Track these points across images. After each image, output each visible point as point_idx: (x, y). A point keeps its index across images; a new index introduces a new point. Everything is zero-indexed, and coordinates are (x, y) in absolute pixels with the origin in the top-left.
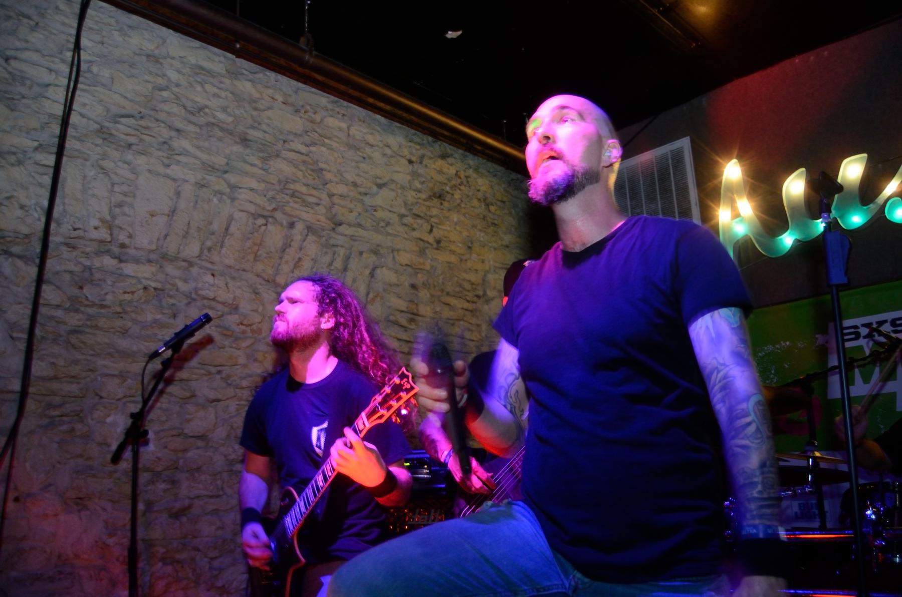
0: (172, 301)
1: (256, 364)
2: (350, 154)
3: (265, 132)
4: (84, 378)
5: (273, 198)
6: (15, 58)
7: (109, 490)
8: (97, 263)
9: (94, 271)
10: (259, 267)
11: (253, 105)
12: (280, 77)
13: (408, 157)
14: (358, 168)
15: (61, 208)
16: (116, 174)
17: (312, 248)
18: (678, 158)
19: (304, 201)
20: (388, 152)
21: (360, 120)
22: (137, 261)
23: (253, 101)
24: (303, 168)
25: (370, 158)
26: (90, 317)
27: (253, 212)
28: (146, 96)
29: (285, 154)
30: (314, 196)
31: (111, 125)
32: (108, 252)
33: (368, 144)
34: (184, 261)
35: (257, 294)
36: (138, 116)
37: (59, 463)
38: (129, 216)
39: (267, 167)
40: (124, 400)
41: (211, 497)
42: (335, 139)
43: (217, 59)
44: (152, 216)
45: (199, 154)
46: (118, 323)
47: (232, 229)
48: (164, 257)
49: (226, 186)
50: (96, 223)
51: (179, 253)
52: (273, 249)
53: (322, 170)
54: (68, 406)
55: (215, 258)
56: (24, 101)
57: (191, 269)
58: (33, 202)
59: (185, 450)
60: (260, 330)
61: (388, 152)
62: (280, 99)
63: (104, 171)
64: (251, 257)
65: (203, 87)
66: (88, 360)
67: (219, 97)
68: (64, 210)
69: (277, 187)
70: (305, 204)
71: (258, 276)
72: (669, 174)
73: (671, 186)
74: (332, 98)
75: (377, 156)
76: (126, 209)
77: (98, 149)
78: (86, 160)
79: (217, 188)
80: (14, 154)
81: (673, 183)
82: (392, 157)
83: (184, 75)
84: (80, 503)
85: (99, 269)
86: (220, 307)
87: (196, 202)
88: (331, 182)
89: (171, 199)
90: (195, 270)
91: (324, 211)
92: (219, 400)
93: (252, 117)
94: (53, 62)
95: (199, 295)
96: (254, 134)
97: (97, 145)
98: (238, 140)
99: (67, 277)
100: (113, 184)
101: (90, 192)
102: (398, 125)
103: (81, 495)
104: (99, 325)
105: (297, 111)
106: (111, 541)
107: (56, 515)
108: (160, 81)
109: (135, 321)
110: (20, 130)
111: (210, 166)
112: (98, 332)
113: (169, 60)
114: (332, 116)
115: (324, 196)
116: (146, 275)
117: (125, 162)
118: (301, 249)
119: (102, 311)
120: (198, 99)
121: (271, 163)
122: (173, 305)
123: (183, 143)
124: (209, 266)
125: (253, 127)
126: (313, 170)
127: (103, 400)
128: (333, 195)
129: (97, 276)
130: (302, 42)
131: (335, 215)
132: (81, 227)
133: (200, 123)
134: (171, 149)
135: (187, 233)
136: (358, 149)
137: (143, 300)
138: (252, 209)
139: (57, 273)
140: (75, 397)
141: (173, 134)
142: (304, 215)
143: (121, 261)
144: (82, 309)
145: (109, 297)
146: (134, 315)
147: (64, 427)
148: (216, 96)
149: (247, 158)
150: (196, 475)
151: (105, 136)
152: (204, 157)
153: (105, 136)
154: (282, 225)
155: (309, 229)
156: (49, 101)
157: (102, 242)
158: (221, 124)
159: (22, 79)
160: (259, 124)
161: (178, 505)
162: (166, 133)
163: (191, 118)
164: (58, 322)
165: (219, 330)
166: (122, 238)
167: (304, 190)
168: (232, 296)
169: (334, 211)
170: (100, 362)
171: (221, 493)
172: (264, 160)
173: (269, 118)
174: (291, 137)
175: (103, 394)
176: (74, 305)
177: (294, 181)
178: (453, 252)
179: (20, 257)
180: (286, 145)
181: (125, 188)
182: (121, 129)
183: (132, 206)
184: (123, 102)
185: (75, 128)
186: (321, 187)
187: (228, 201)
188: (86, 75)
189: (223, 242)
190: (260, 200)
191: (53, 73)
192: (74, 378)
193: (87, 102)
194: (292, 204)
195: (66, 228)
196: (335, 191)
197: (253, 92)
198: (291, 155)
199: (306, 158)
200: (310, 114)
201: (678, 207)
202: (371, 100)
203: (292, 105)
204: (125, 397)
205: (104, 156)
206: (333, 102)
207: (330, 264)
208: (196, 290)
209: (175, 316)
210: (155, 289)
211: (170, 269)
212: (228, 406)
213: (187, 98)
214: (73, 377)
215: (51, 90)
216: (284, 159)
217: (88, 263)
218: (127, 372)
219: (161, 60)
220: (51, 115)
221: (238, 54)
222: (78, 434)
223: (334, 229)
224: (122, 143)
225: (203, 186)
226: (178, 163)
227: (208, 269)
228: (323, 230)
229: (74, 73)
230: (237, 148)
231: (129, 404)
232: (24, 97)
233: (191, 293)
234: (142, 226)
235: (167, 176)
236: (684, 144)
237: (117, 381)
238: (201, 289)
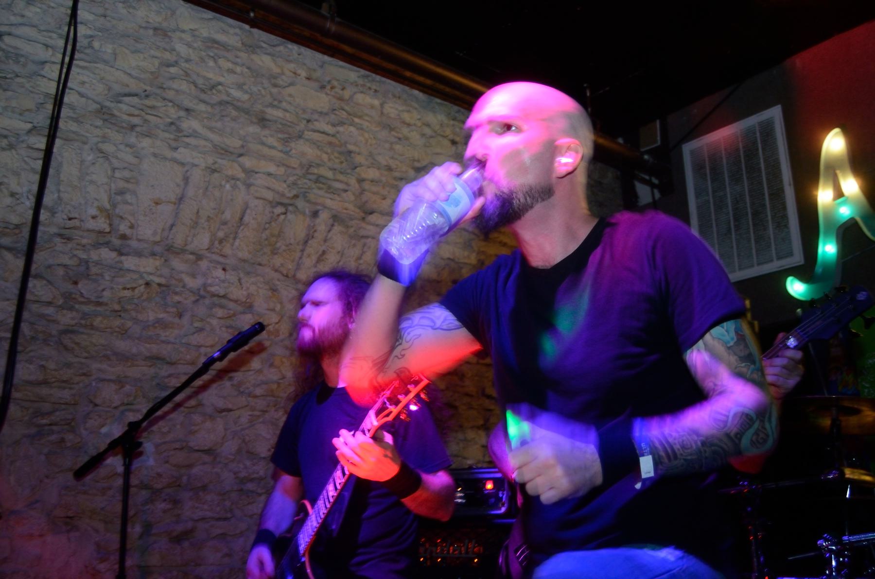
0: (177, 298)
1: (273, 370)
2: (384, 134)
3: (286, 111)
4: (78, 383)
5: (295, 184)
6: (9, 34)
7: (102, 509)
8: (94, 255)
9: (91, 265)
10: (277, 261)
11: (273, 81)
12: (304, 50)
13: (451, 137)
14: (391, 149)
15: (56, 195)
16: (117, 158)
17: (338, 240)
18: (767, 129)
19: (329, 187)
20: (428, 131)
21: (394, 96)
22: (139, 254)
23: (272, 77)
24: (329, 151)
25: (407, 139)
26: (85, 316)
27: (271, 199)
28: (152, 73)
29: (308, 134)
30: (341, 182)
31: (112, 105)
32: (107, 244)
33: (404, 123)
34: (192, 253)
35: (274, 290)
36: (143, 94)
37: (47, 477)
38: (131, 204)
39: (288, 149)
40: (122, 408)
41: (219, 519)
42: (367, 118)
43: (232, 31)
44: (157, 204)
45: (211, 135)
46: (117, 322)
47: (246, 219)
48: (170, 249)
49: (240, 170)
50: (93, 211)
51: (186, 245)
52: (292, 241)
53: (350, 152)
54: (58, 413)
55: (227, 250)
56: (18, 80)
57: (199, 262)
58: (25, 189)
59: (190, 466)
60: (278, 331)
61: (428, 131)
62: (303, 74)
63: (106, 156)
64: (267, 250)
65: (215, 62)
66: (81, 363)
67: (235, 73)
68: (60, 198)
69: (299, 172)
70: (330, 190)
71: (276, 271)
72: (757, 150)
73: (759, 164)
74: (363, 72)
75: (415, 136)
76: (128, 197)
77: (98, 132)
78: (85, 143)
79: (230, 173)
80: (6, 137)
81: (762, 161)
82: (431, 137)
83: (195, 49)
84: (67, 523)
85: (97, 263)
86: (232, 305)
87: (207, 188)
88: (361, 165)
89: (178, 185)
90: (204, 264)
91: (352, 198)
92: (230, 410)
93: (271, 94)
94: (50, 37)
95: (208, 292)
96: (273, 113)
97: (97, 127)
98: (255, 120)
99: (61, 272)
100: (114, 170)
101: (88, 178)
102: (439, 101)
103: (70, 514)
104: (95, 324)
105: (323, 87)
106: (102, 567)
107: (41, 536)
108: (167, 56)
109: (136, 321)
110: (13, 112)
111: (223, 149)
112: (92, 332)
113: (178, 34)
114: (362, 92)
115: (353, 181)
116: (149, 269)
117: (127, 145)
118: (325, 241)
119: (99, 309)
120: (210, 75)
121: (293, 145)
122: (179, 302)
123: (191, 124)
124: (221, 259)
125: (271, 105)
126: (340, 153)
127: (97, 408)
128: (363, 180)
129: (94, 270)
130: (325, 10)
131: (366, 202)
132: (77, 216)
133: (212, 102)
134: (179, 130)
135: (196, 223)
136: (392, 129)
137: (145, 297)
138: (269, 195)
139: (49, 267)
140: (66, 404)
141: (182, 113)
142: (329, 203)
143: (121, 254)
144: (77, 306)
145: (107, 294)
146: (134, 314)
147: (53, 437)
148: (231, 71)
149: (264, 139)
150: (201, 493)
151: (106, 117)
152: (216, 138)
153: (106, 117)
154: (304, 214)
155: (336, 218)
156: (45, 80)
157: (101, 232)
158: (235, 102)
159: (17, 56)
160: (280, 102)
161: (179, 528)
162: (173, 113)
163: (203, 96)
164: (49, 321)
165: (230, 330)
166: (123, 228)
167: (330, 174)
168: (245, 293)
169: (364, 198)
170: (95, 366)
171: (229, 515)
172: (286, 141)
173: (290, 95)
174: (316, 116)
175: (98, 401)
176: (69, 301)
177: (318, 165)
178: (504, 245)
179: (9, 249)
180: (310, 126)
181: (126, 174)
182: (122, 110)
183: (134, 193)
184: (125, 79)
185: (72, 108)
186: (349, 171)
187: (243, 188)
188: (87, 51)
189: (236, 233)
190: (281, 187)
191: (50, 49)
192: (66, 383)
193: (86, 79)
194: (316, 191)
195: (60, 218)
196: (364, 176)
197: (272, 65)
198: (316, 136)
199: (330, 139)
200: (336, 90)
201: (769, 188)
202: (408, 74)
203: (317, 80)
204: (123, 404)
205: (105, 139)
206: (364, 76)
207: (359, 258)
208: (205, 286)
209: (180, 316)
210: (159, 285)
211: (177, 263)
212: (239, 417)
213: (198, 75)
214: (64, 382)
215: (47, 67)
216: (307, 140)
217: (84, 256)
218: (126, 377)
219: (169, 34)
220: (47, 95)
221: (253, 24)
222: (69, 444)
223: (363, 219)
224: (124, 125)
225: (214, 171)
226: (187, 146)
227: (219, 263)
228: (352, 219)
229: (69, 48)
230: (253, 129)
231: (127, 413)
232: (17, 76)
233: (199, 290)
234: (145, 215)
235: (175, 161)
236: (775, 113)
237: (114, 387)
238: (211, 285)
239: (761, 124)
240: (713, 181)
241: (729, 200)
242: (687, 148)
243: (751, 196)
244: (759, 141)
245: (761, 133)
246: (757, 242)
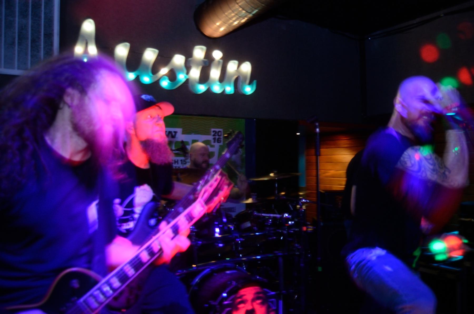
72: (41, 5)
201: (44, 30)
240: (6, 8)
241: (17, 25)
243: (32, 30)
246: (32, 56)
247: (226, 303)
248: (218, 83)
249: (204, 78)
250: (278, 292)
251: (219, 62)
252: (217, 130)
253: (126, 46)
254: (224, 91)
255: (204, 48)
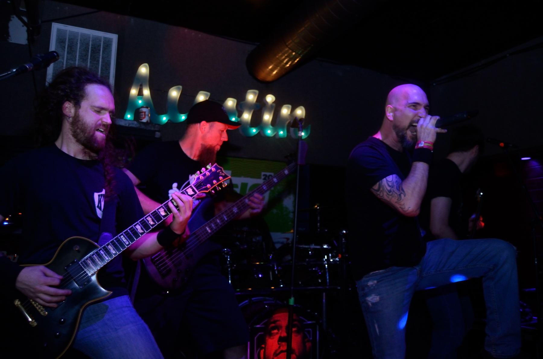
18: (108, 44)
72: (100, 50)
73: (99, 58)
81: (101, 57)
236: (114, 38)
239: (105, 38)
240: (68, 53)
242: (56, 27)
244: (102, 46)
245: (104, 43)
247: (258, 326)
248: (271, 127)
249: (257, 121)
250: (314, 322)
251: (271, 106)
252: (268, 174)
253: (178, 89)
254: (277, 134)
255: (257, 92)
